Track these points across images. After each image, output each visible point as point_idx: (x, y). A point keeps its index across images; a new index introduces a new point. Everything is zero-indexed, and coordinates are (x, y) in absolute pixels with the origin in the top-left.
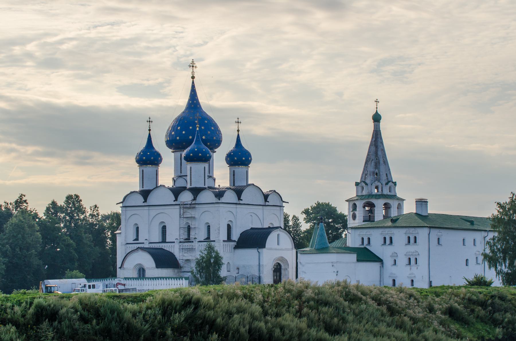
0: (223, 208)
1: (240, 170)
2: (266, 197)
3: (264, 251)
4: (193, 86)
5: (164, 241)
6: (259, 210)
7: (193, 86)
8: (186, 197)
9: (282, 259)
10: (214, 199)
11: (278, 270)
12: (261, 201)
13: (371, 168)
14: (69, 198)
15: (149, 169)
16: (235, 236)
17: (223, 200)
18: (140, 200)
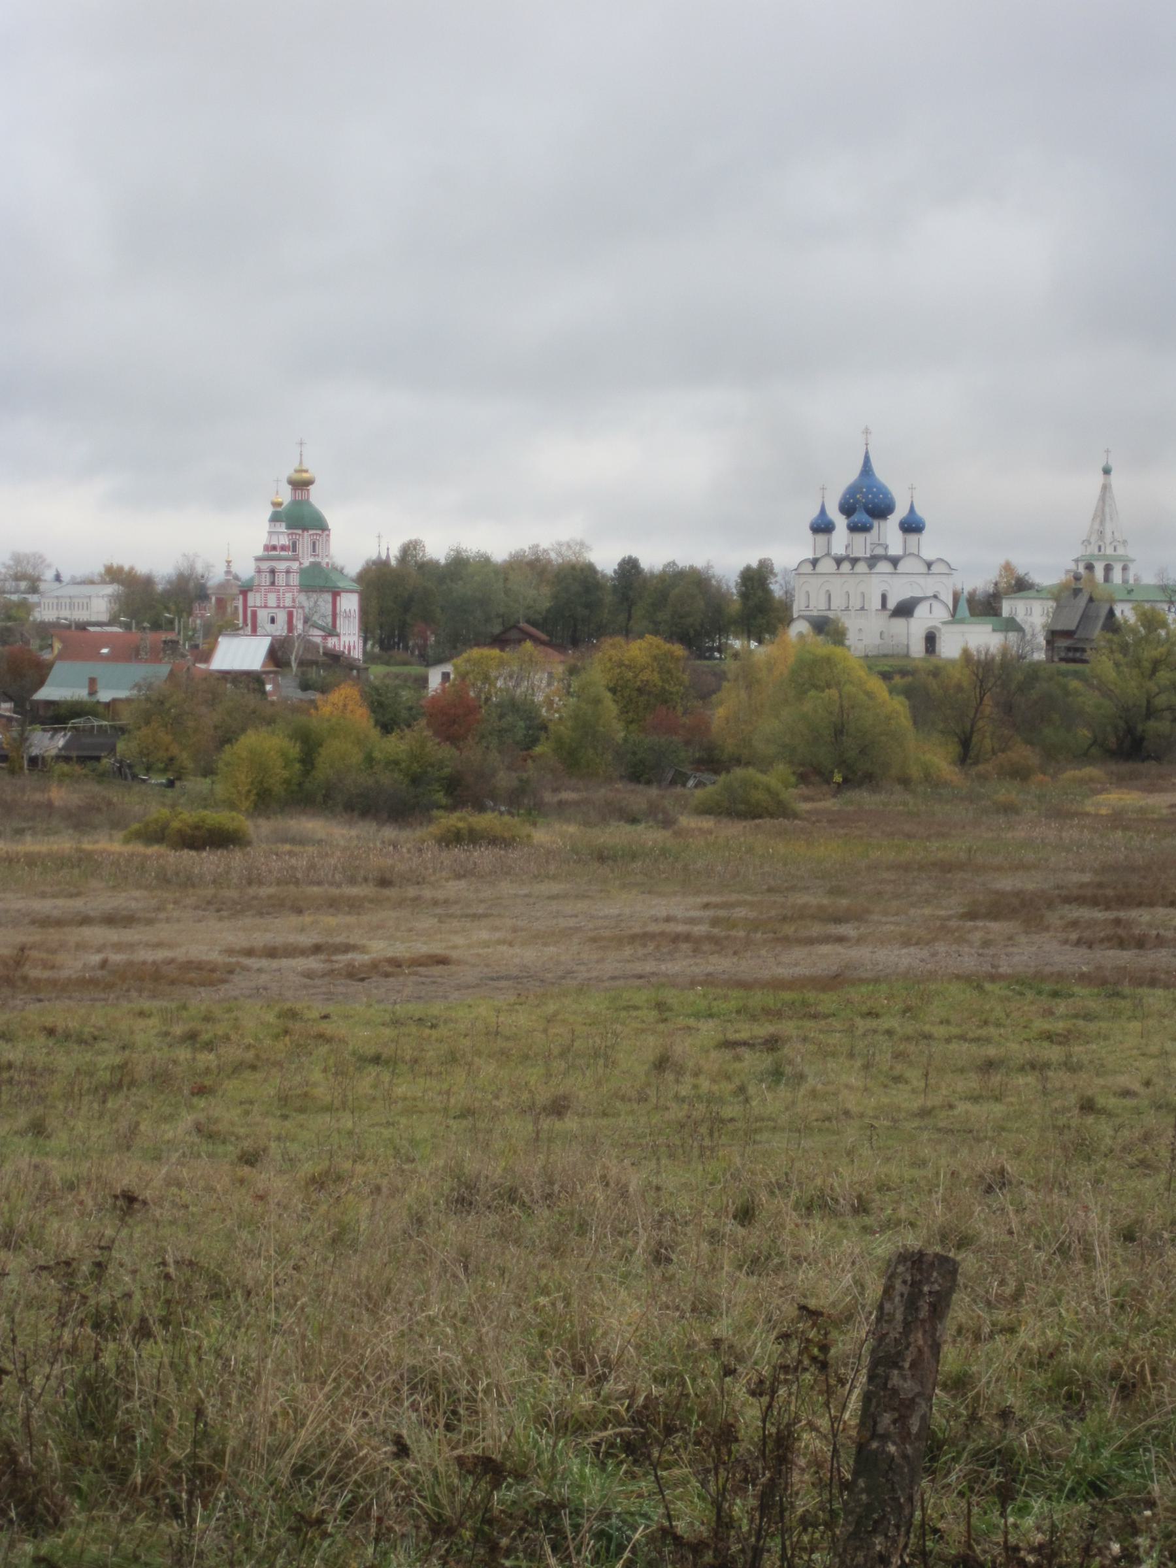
0: (875, 580)
1: (913, 538)
2: (929, 565)
3: (912, 621)
4: (867, 453)
5: (829, 609)
6: (921, 580)
7: (867, 453)
8: (846, 567)
9: (935, 627)
10: (866, 570)
11: (931, 640)
12: (924, 569)
13: (1096, 526)
14: (760, 562)
15: (822, 538)
16: (892, 604)
17: (875, 570)
18: (808, 568)
